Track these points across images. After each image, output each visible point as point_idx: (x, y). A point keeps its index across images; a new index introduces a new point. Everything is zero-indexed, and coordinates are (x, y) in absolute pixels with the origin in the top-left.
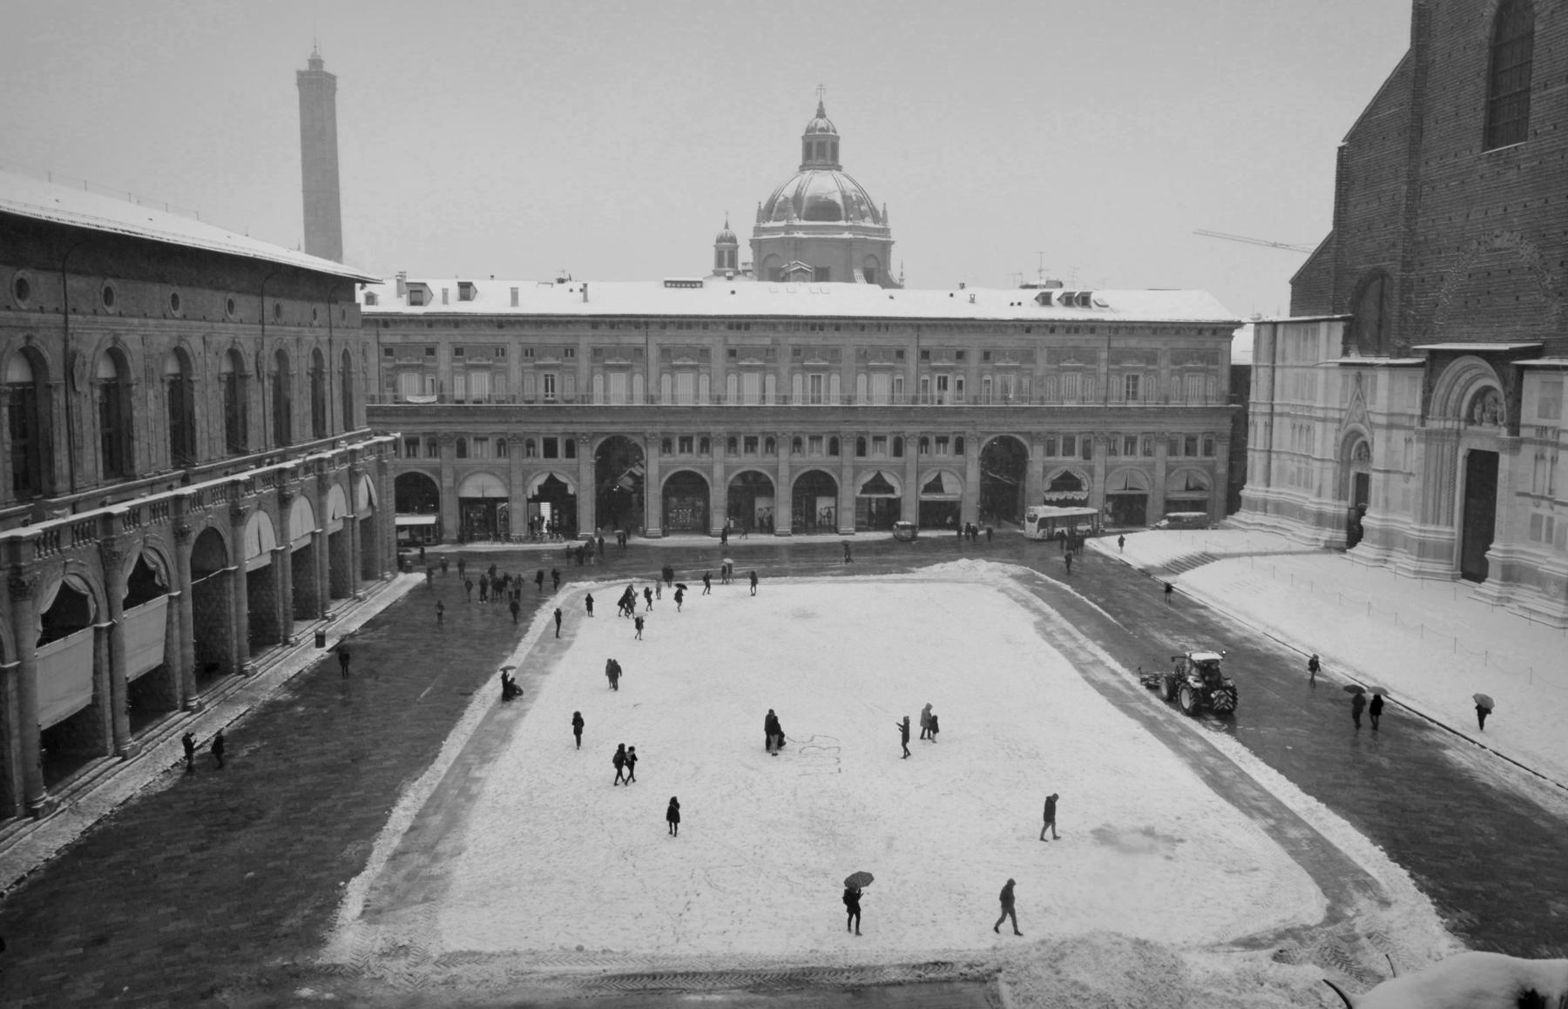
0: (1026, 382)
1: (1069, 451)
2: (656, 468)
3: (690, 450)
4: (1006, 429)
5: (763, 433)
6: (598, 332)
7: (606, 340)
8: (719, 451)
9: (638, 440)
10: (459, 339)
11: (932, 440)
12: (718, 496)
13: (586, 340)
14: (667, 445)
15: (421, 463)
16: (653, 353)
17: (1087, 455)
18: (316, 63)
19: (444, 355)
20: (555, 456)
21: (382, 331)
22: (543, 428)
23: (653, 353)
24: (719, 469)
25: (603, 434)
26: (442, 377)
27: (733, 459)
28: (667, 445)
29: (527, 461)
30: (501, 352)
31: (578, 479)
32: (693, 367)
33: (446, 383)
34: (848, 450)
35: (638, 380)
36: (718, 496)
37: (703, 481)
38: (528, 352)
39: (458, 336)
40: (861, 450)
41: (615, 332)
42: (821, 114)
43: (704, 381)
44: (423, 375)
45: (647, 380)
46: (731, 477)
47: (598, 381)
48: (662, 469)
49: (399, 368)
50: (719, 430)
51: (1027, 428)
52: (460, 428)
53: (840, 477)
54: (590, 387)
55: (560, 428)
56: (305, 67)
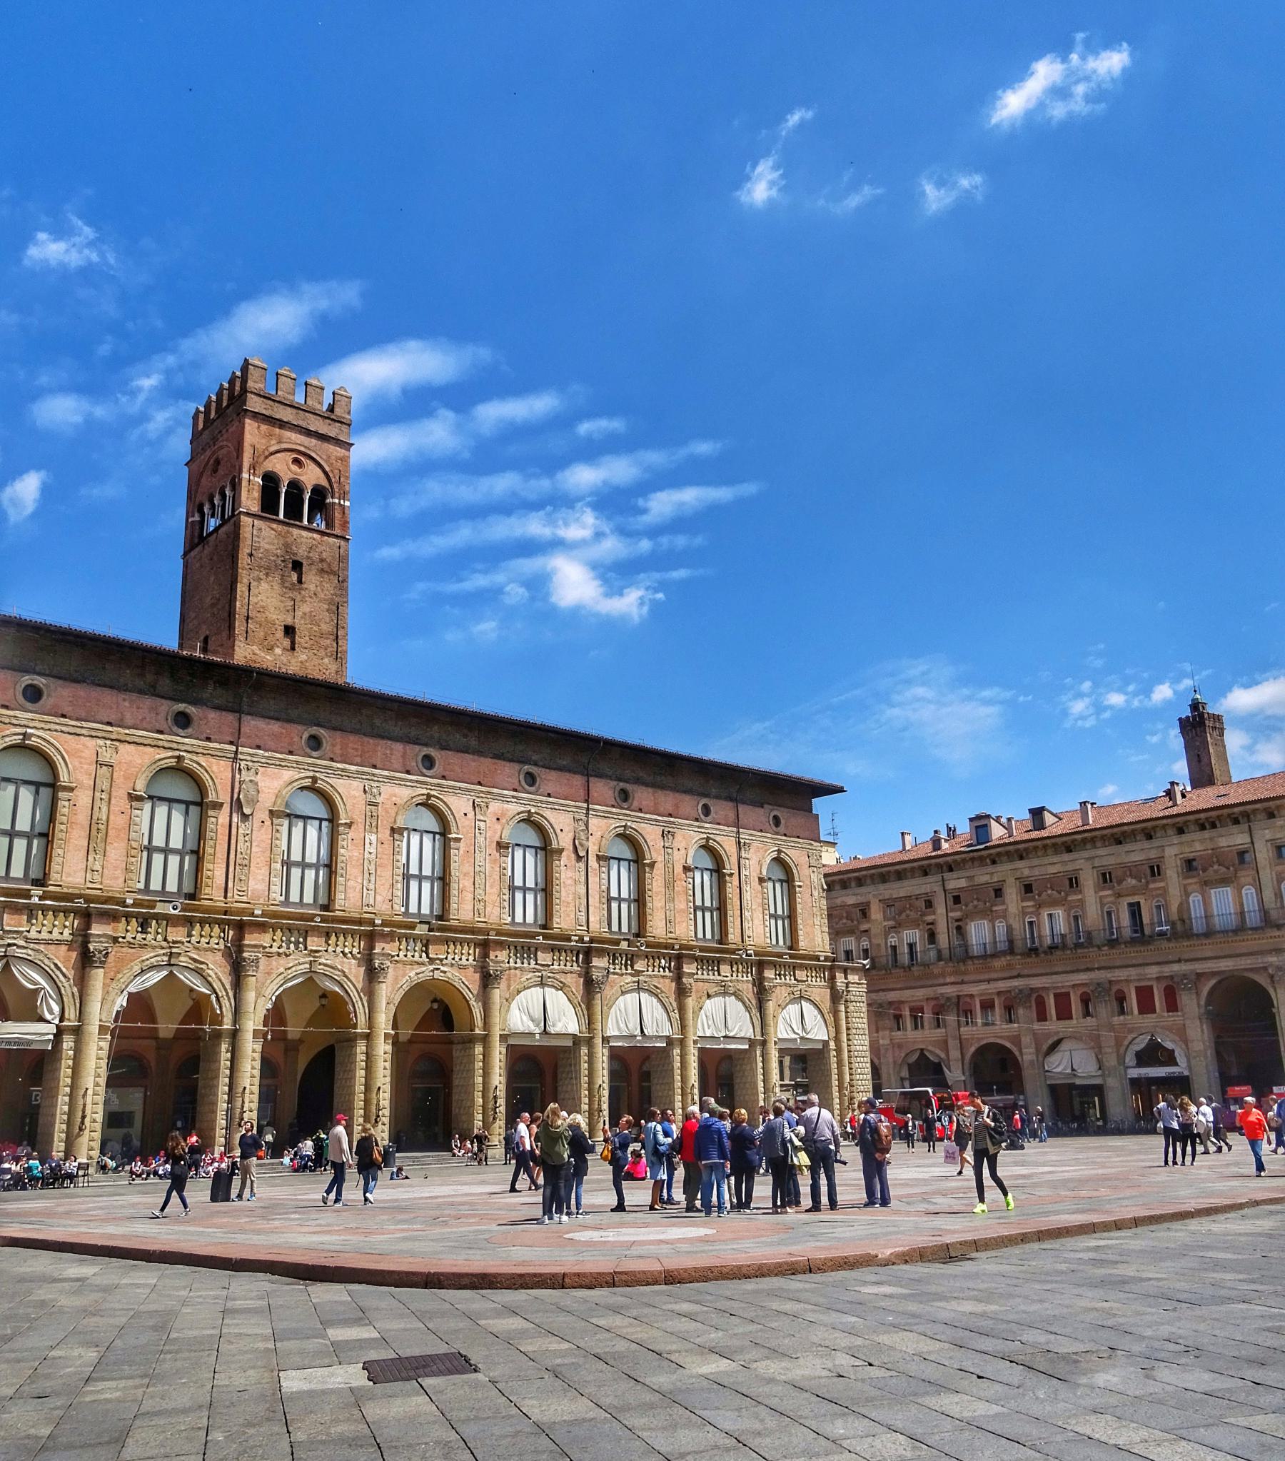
6: (1185, 838)
7: (1198, 846)
9: (1262, 980)
10: (1026, 872)
13: (1172, 851)
16: (1263, 853)
19: (1012, 894)
20: (1152, 1010)
21: (947, 875)
22: (1132, 973)
23: (1263, 853)
25: (1214, 974)
26: (1011, 921)
30: (1073, 882)
31: (1186, 1041)
33: (1016, 925)
35: (1249, 892)
38: (1106, 878)
39: (1025, 868)
41: (1206, 834)
44: (992, 921)
45: (1260, 891)
47: (1195, 899)
52: (1036, 982)
54: (1184, 907)
55: (1153, 971)
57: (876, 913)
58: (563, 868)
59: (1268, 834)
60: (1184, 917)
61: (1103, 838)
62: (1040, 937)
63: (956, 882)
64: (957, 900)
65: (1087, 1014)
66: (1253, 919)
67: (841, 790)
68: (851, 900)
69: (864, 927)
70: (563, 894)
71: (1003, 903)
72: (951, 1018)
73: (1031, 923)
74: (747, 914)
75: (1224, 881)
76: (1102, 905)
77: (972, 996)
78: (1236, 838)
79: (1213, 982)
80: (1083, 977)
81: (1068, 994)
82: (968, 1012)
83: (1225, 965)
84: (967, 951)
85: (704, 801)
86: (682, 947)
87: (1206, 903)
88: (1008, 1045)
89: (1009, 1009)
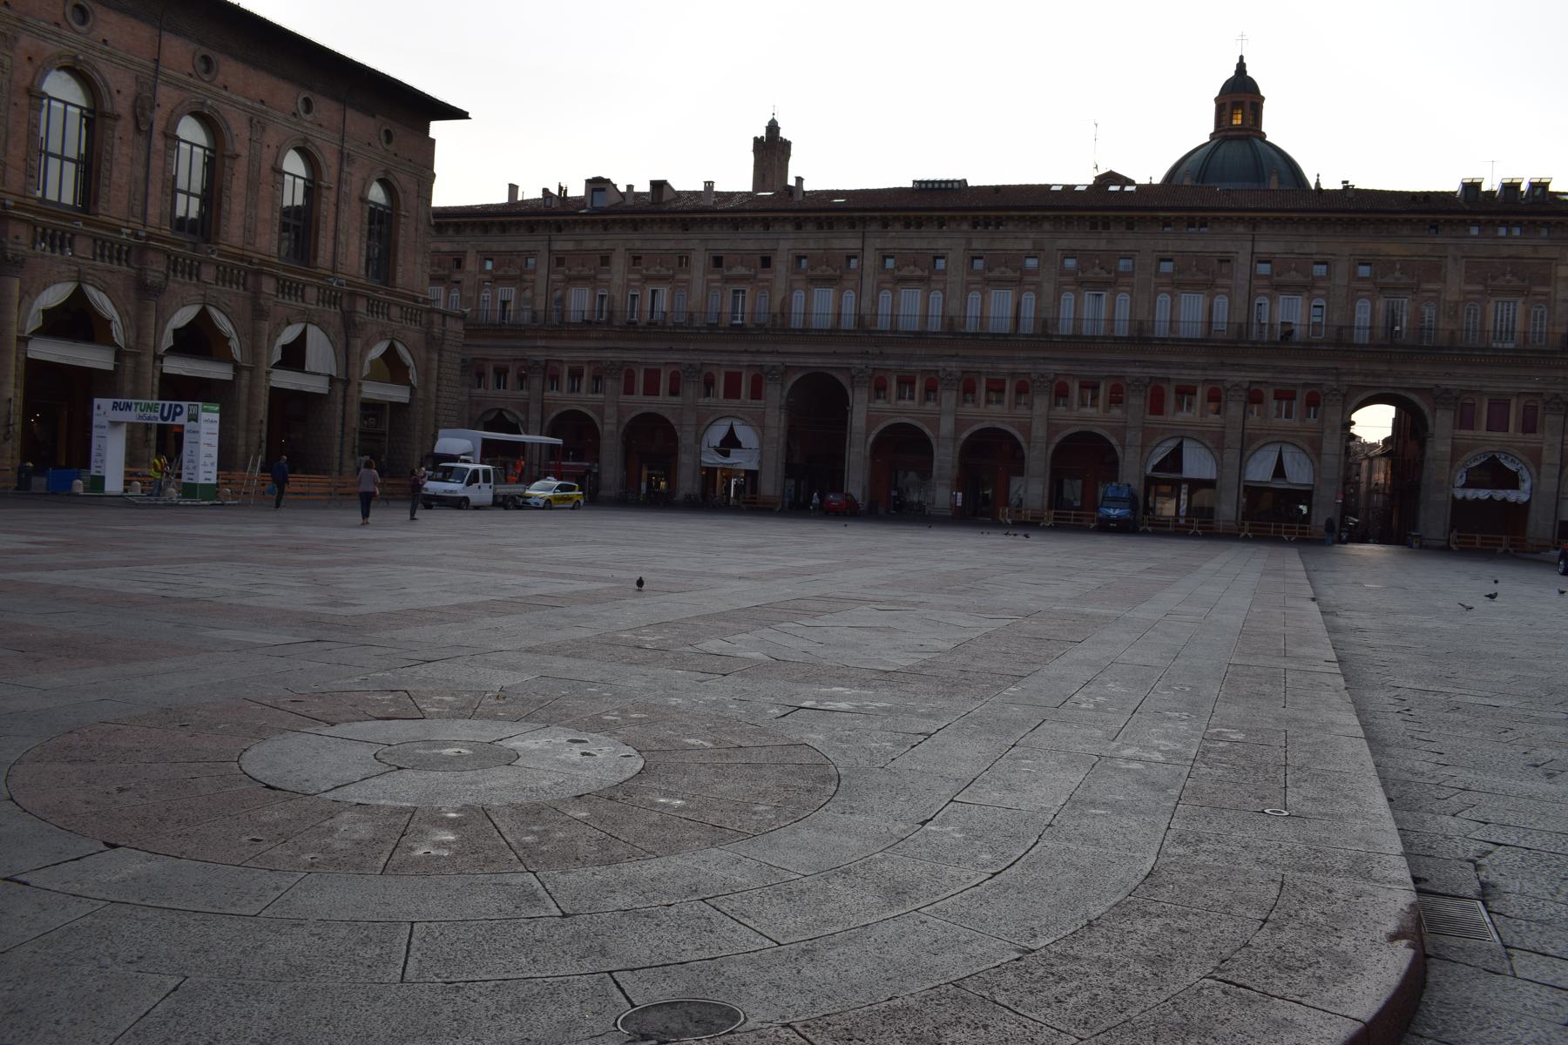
0: (1429, 312)
1: (1498, 422)
2: (865, 416)
3: (912, 398)
4: (1390, 381)
5: (1013, 375)
8: (948, 398)
9: (843, 379)
10: (638, 244)
11: (1269, 393)
12: (945, 458)
14: (880, 389)
15: (583, 399)
17: (1529, 426)
18: (773, 128)
19: (619, 263)
23: (871, 259)
24: (947, 423)
25: (801, 368)
27: (969, 408)
28: (880, 389)
29: (703, 401)
30: (683, 260)
32: (921, 280)
34: (1137, 402)
35: (849, 297)
36: (945, 458)
37: (927, 441)
39: (637, 241)
40: (1157, 407)
42: (1241, 67)
43: (936, 297)
45: (859, 298)
46: (965, 435)
47: (798, 298)
48: (871, 421)
49: (570, 280)
50: (1038, 424)
51: (1426, 383)
52: (627, 356)
53: (1123, 447)
54: (786, 303)
55: (745, 359)
56: (762, 133)
57: (470, 264)
58: (117, 141)
59: (878, 243)
60: (785, 311)
61: (724, 220)
62: (640, 311)
63: (562, 244)
64: (560, 262)
65: (674, 392)
66: (848, 323)
67: (463, 115)
68: (446, 247)
69: (457, 277)
70: (115, 174)
71: (609, 272)
72: (536, 383)
73: (633, 297)
74: (342, 238)
75: (827, 281)
76: (708, 288)
77: (561, 362)
78: (847, 241)
79: (799, 376)
80: (676, 357)
81: (659, 371)
82: (554, 379)
83: (813, 362)
84: (563, 316)
85: (307, 94)
86: (262, 262)
87: (808, 302)
88: (591, 414)
89: (597, 379)
